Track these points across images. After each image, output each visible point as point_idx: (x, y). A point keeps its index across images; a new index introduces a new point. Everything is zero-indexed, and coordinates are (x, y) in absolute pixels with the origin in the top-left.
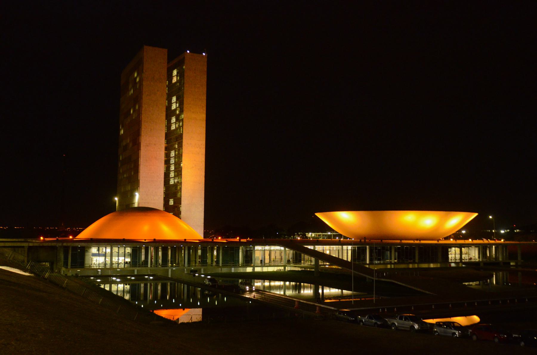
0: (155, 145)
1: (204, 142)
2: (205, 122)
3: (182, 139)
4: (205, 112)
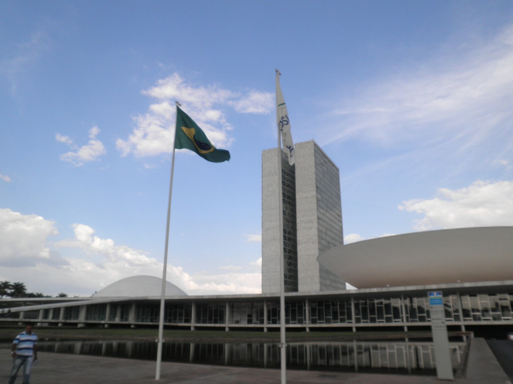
0: (273, 228)
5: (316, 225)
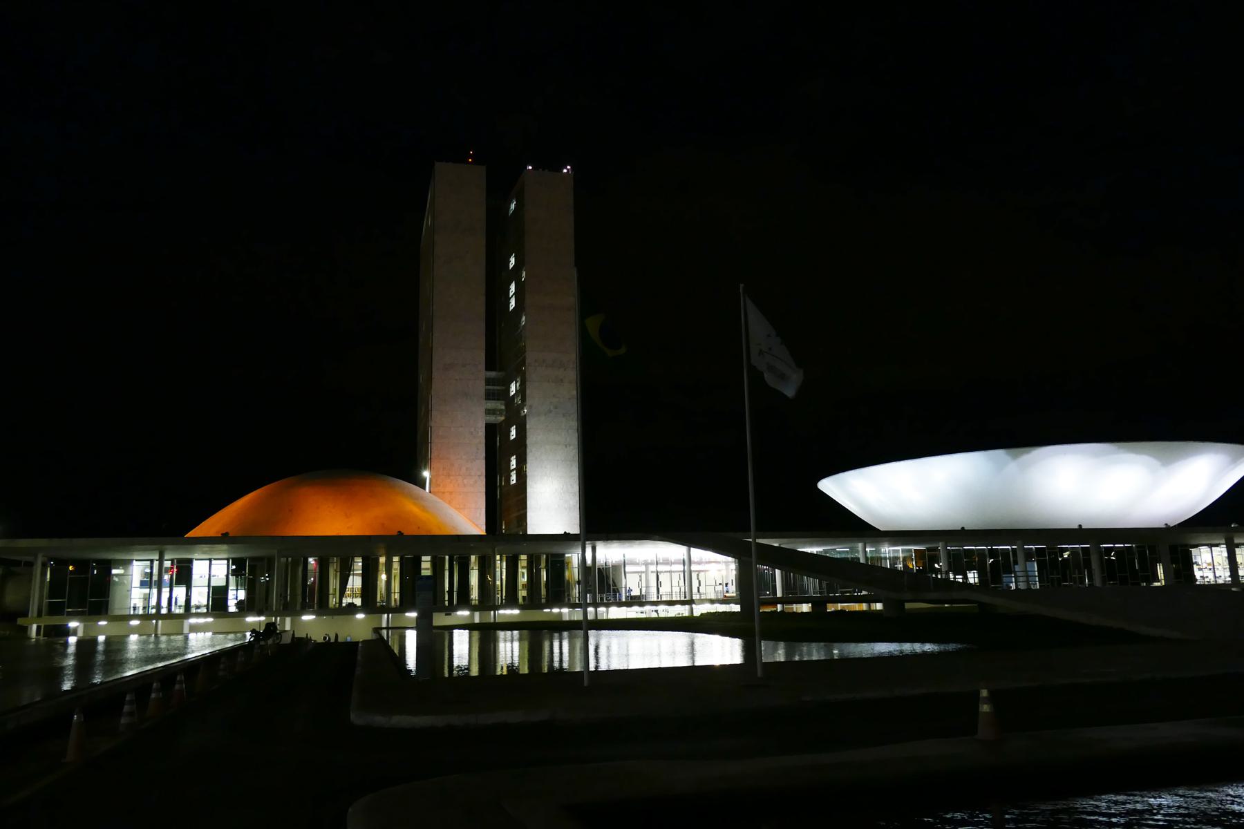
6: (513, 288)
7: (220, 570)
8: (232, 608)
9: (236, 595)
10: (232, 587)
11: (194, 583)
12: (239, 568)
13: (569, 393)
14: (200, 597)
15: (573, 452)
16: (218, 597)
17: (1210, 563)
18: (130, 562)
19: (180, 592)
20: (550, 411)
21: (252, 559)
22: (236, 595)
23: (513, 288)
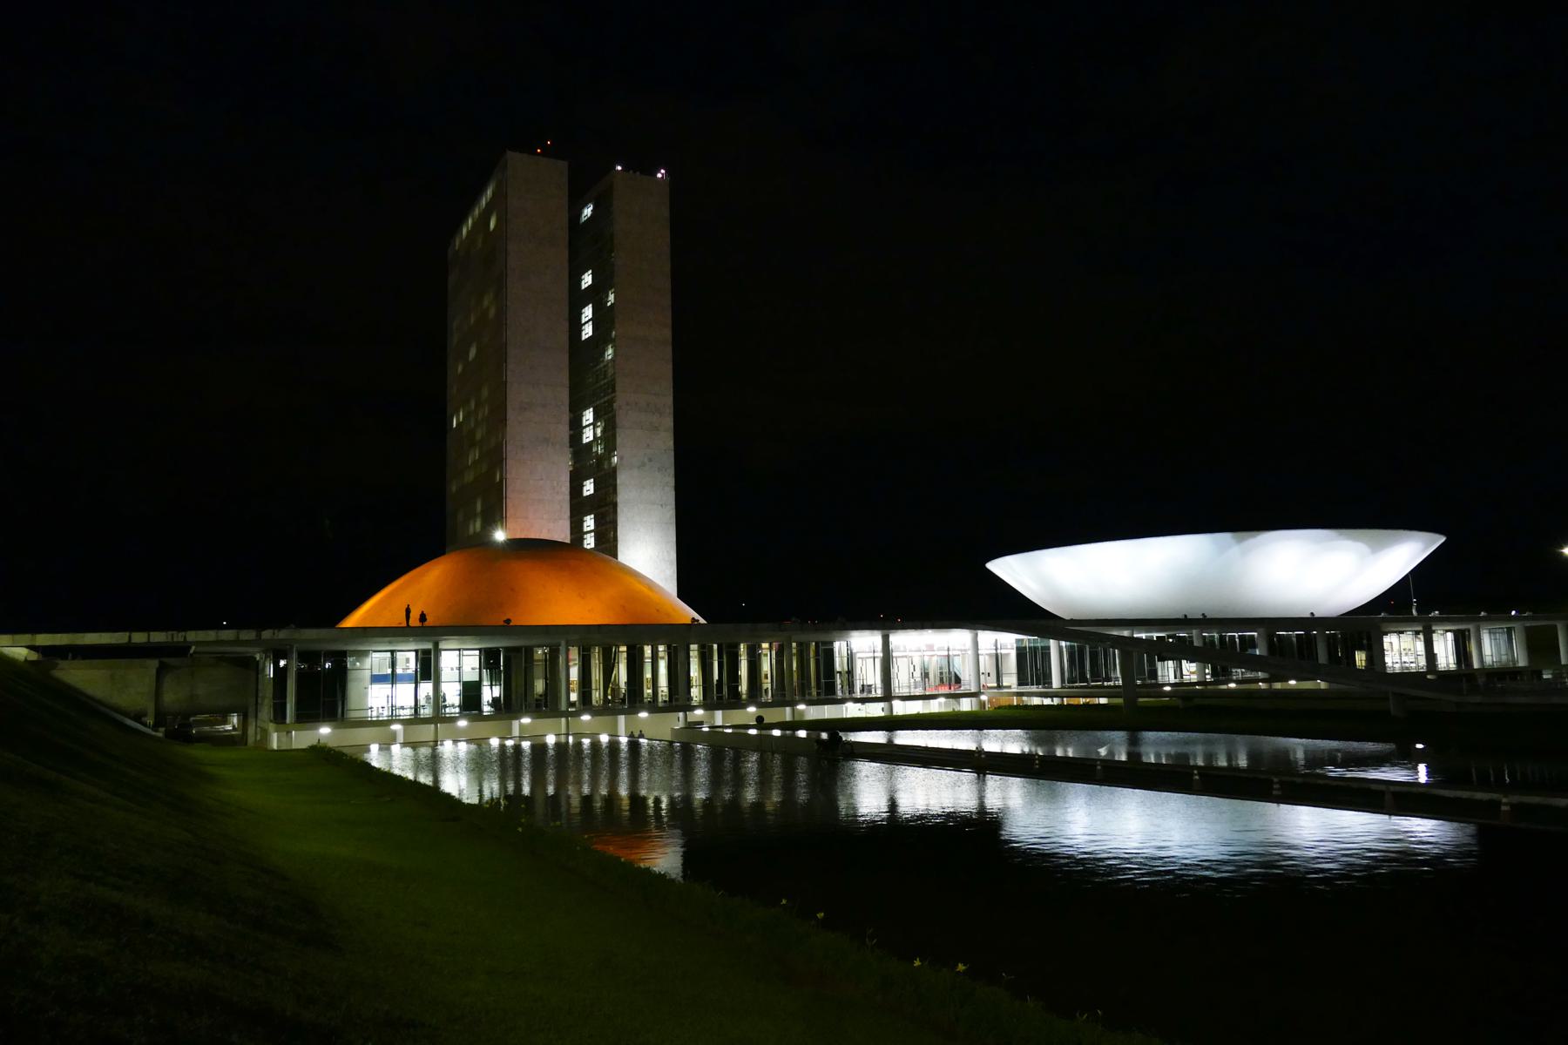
1: (669, 400)
2: (669, 349)
3: (614, 391)
4: (669, 321)
5: (669, 422)
6: (588, 312)
7: (470, 663)
8: (487, 709)
9: (490, 693)
10: (486, 683)
11: (444, 677)
12: (489, 659)
13: (665, 442)
14: (452, 694)
15: (669, 513)
16: (471, 694)
17: (1402, 650)
18: (365, 653)
19: (426, 688)
20: (643, 465)
21: (507, 649)
22: (490, 693)
23: (588, 312)
